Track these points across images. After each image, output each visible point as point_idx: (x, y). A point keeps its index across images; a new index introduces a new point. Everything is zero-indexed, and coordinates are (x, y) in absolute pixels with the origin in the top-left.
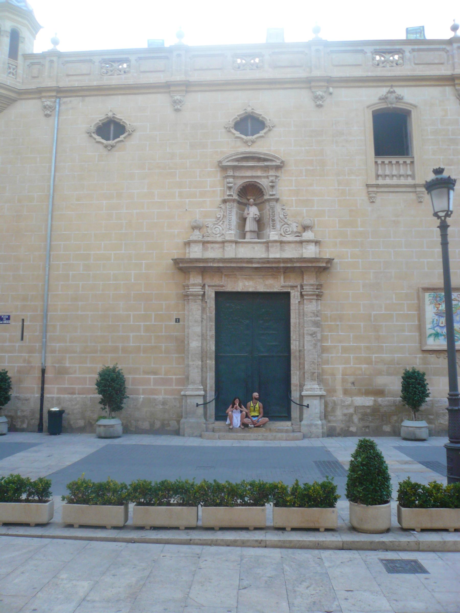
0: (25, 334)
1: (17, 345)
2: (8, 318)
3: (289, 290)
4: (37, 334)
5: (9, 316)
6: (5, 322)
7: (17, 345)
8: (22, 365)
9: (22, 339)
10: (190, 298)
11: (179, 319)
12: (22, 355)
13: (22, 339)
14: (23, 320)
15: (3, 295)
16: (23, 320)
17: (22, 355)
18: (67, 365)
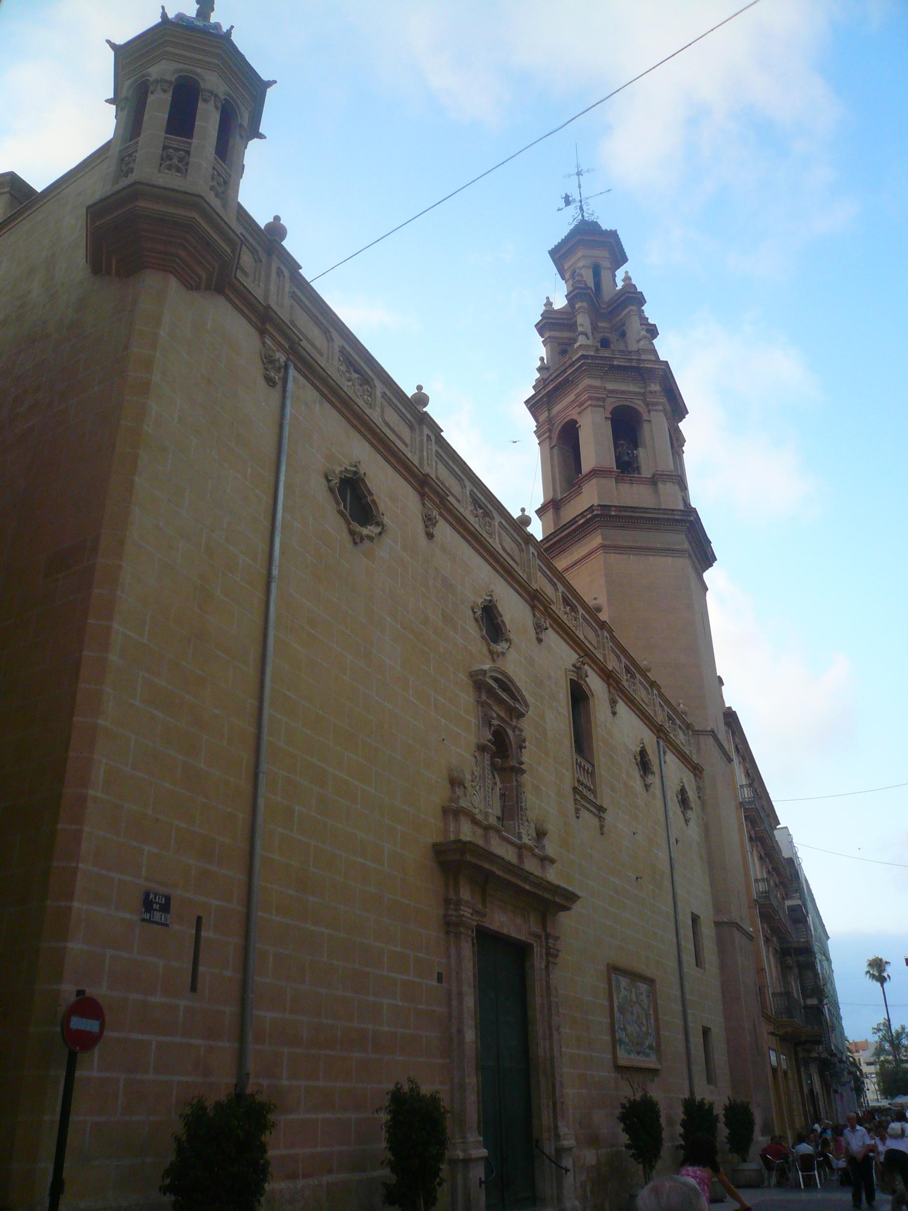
0: (201, 969)
1: (183, 1003)
2: (165, 908)
3: (532, 942)
4: (229, 973)
5: (168, 899)
6: (157, 916)
7: (183, 1003)
8: (190, 1079)
9: (193, 988)
10: (462, 930)
11: (441, 974)
12: (193, 1041)
13: (193, 988)
14: (199, 919)
15: (157, 820)
16: (199, 919)
17: (193, 1041)
18: (285, 1082)
